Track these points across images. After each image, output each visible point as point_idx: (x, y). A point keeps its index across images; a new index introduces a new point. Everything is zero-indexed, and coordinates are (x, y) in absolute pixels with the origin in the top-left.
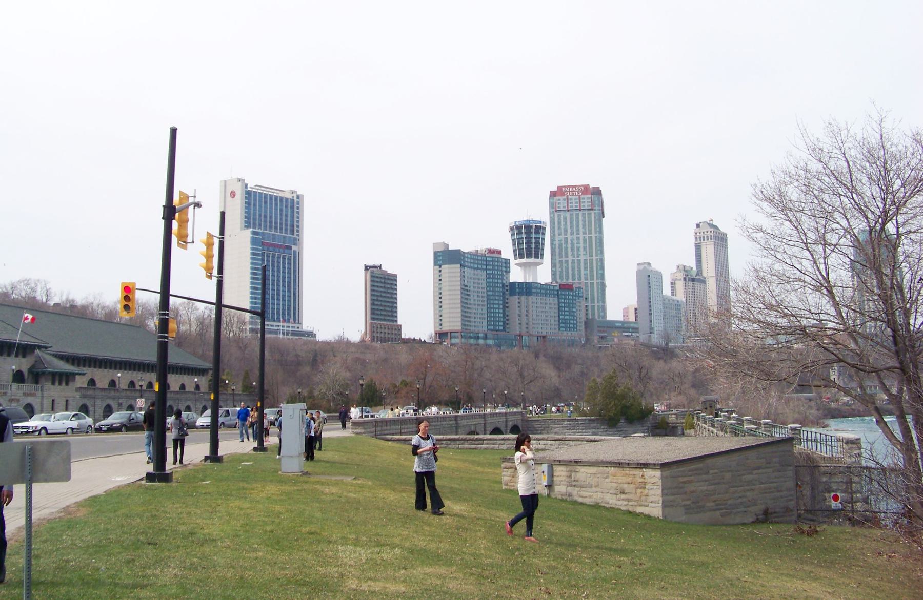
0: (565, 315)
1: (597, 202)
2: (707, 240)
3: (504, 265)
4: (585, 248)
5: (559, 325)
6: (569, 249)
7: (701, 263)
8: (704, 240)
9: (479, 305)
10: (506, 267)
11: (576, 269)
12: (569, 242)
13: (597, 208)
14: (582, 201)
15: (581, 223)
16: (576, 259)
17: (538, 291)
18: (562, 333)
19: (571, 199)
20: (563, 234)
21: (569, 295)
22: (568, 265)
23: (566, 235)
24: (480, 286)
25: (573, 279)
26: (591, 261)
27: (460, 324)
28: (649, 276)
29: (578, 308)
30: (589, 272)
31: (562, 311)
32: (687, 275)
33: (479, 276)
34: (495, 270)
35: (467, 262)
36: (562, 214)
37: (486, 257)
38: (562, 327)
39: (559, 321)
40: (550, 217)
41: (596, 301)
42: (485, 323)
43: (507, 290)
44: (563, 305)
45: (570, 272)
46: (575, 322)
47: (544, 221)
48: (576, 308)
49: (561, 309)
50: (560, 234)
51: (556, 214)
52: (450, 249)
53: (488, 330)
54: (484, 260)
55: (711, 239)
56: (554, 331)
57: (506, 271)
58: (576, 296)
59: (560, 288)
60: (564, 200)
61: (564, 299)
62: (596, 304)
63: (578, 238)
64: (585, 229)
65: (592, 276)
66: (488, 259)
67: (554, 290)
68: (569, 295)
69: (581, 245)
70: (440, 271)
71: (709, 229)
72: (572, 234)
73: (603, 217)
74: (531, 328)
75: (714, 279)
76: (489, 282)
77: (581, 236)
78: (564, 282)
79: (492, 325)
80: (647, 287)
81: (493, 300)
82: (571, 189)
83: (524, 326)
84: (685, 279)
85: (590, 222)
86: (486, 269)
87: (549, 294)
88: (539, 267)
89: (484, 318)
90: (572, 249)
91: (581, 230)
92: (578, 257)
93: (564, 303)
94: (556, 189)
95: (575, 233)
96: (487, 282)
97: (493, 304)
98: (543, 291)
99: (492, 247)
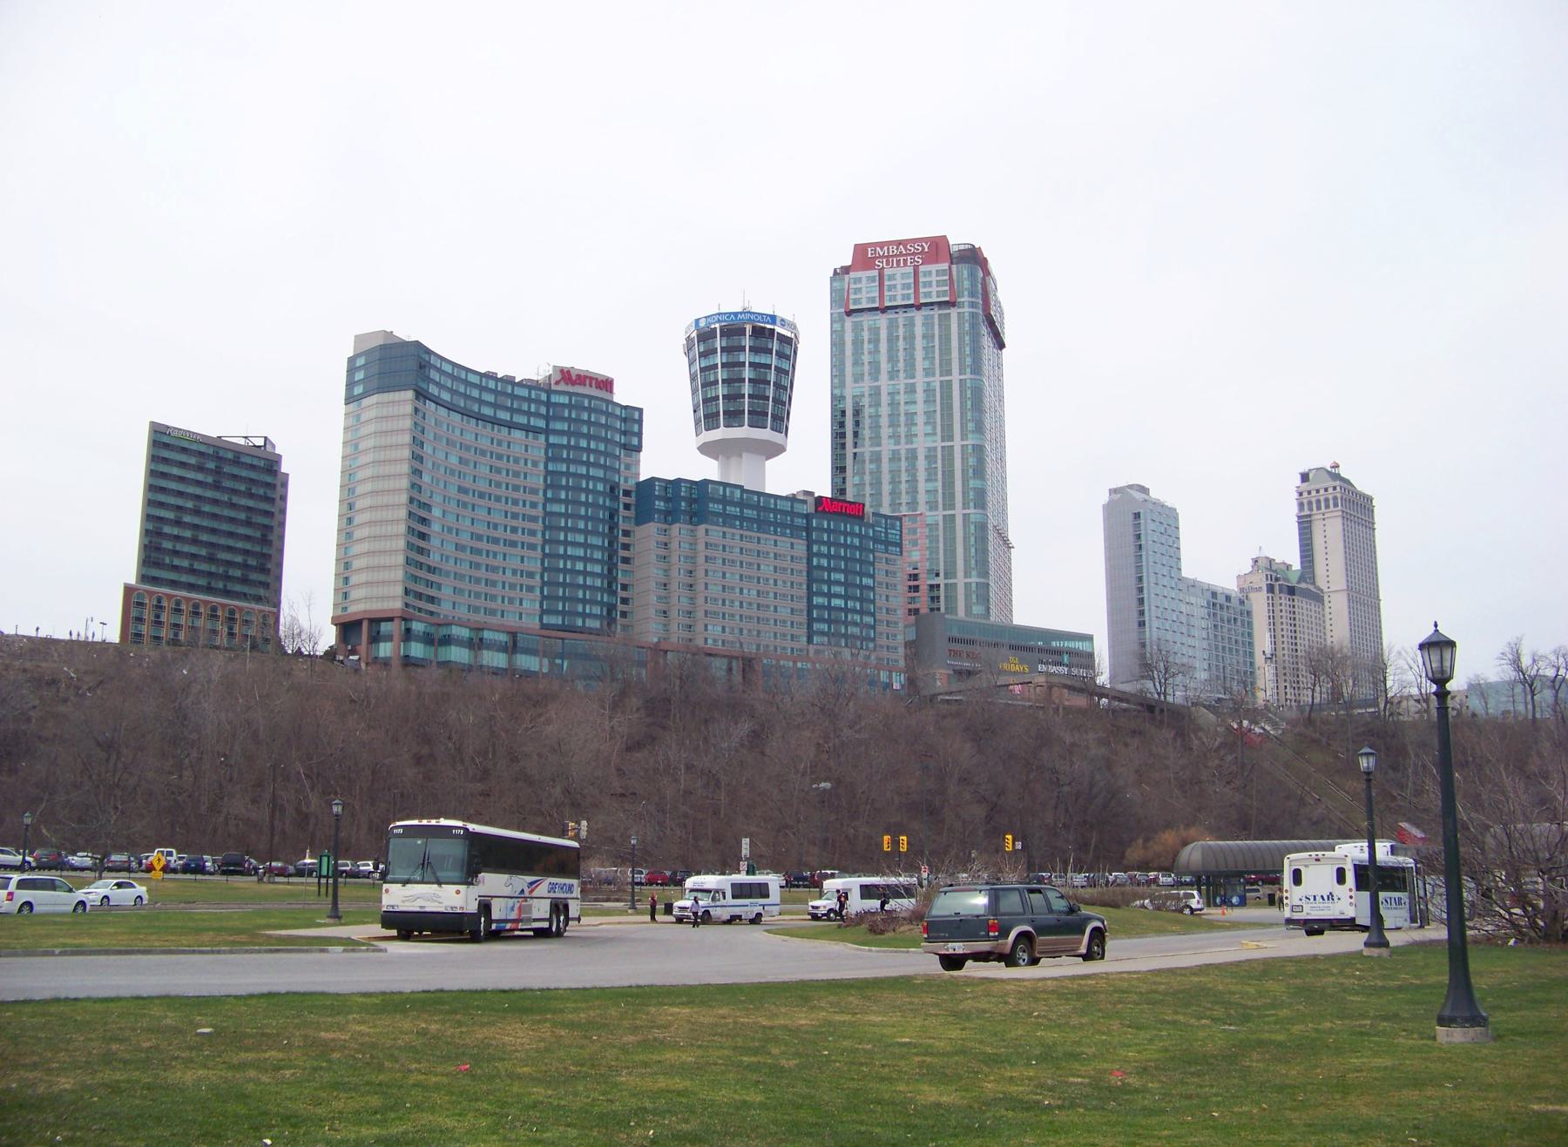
0: (830, 596)
1: (966, 284)
2: (1327, 506)
4: (929, 415)
5: (810, 626)
6: (884, 421)
7: (1312, 561)
8: (1319, 508)
9: (513, 544)
11: (904, 477)
12: (885, 399)
14: (922, 279)
15: (919, 343)
16: (903, 448)
17: (734, 510)
18: (817, 652)
19: (892, 277)
20: (866, 377)
21: (846, 534)
22: (879, 467)
23: (877, 379)
24: (520, 481)
25: (895, 505)
26: (948, 452)
27: (399, 590)
28: (1137, 516)
29: (881, 577)
30: (939, 484)
31: (823, 581)
32: (1277, 579)
33: (517, 450)
34: (579, 435)
36: (866, 320)
37: (549, 392)
38: (822, 633)
39: (809, 613)
40: (832, 332)
41: (960, 573)
42: (531, 604)
43: (627, 507)
44: (824, 562)
45: (886, 488)
46: (868, 620)
47: (788, 317)
48: (873, 576)
49: (816, 573)
50: (858, 378)
51: (849, 322)
54: (538, 402)
55: (1336, 505)
56: (789, 644)
57: (624, 447)
58: (876, 540)
59: (816, 510)
60: (872, 279)
61: (829, 544)
62: (960, 580)
63: (911, 389)
64: (933, 363)
66: (555, 399)
67: (792, 514)
68: (846, 534)
69: (920, 408)
71: (1331, 483)
72: (893, 374)
74: (699, 627)
75: (1345, 594)
76: (552, 473)
77: (920, 380)
79: (557, 613)
80: (1132, 549)
81: (566, 529)
82: (893, 250)
83: (677, 620)
84: (1271, 589)
85: (945, 339)
86: (547, 432)
87: (776, 524)
89: (530, 589)
90: (894, 424)
91: (920, 364)
92: (909, 442)
93: (829, 557)
95: (902, 375)
96: (548, 472)
97: (566, 543)
98: (748, 513)
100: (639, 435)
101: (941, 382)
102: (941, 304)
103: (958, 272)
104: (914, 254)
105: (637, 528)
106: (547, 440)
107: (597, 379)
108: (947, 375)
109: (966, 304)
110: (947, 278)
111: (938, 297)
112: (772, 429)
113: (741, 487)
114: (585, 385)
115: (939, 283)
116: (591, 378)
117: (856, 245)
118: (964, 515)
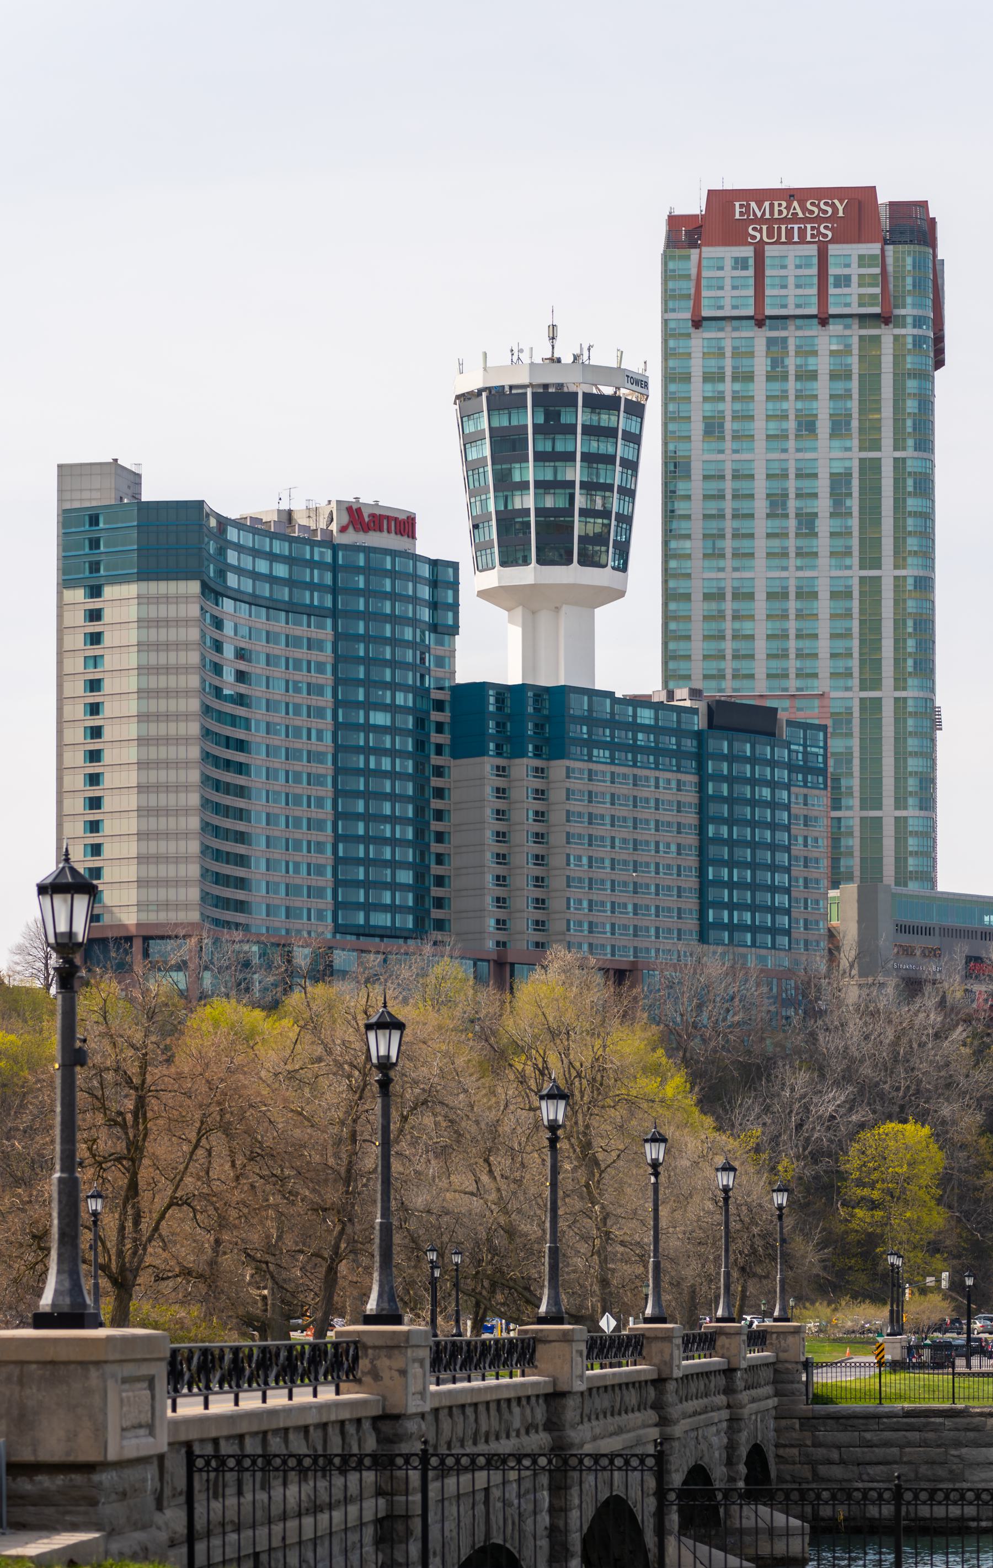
3: (425, 592)
10: (434, 606)
13: (908, 311)
14: (833, 270)
35: (239, 571)
36: (728, 338)
37: (335, 548)
43: (440, 727)
51: (698, 342)
52: (145, 497)
53: (338, 929)
57: (434, 628)
59: (711, 725)
60: (740, 263)
65: (871, 664)
67: (679, 732)
70: (95, 615)
73: (939, 363)
78: (728, 689)
82: (780, 207)
88: (603, 614)
94: (695, 205)
99: (367, 499)
100: (455, 607)
101: (862, 461)
102: (862, 317)
103: (896, 260)
104: (819, 220)
105: (453, 762)
106: (335, 627)
107: (396, 519)
108: (871, 449)
109: (909, 320)
110: (877, 270)
111: (860, 305)
112: (613, 568)
113: (610, 695)
114: (381, 530)
115: (862, 282)
116: (388, 518)
117: (710, 192)
118: (897, 699)
